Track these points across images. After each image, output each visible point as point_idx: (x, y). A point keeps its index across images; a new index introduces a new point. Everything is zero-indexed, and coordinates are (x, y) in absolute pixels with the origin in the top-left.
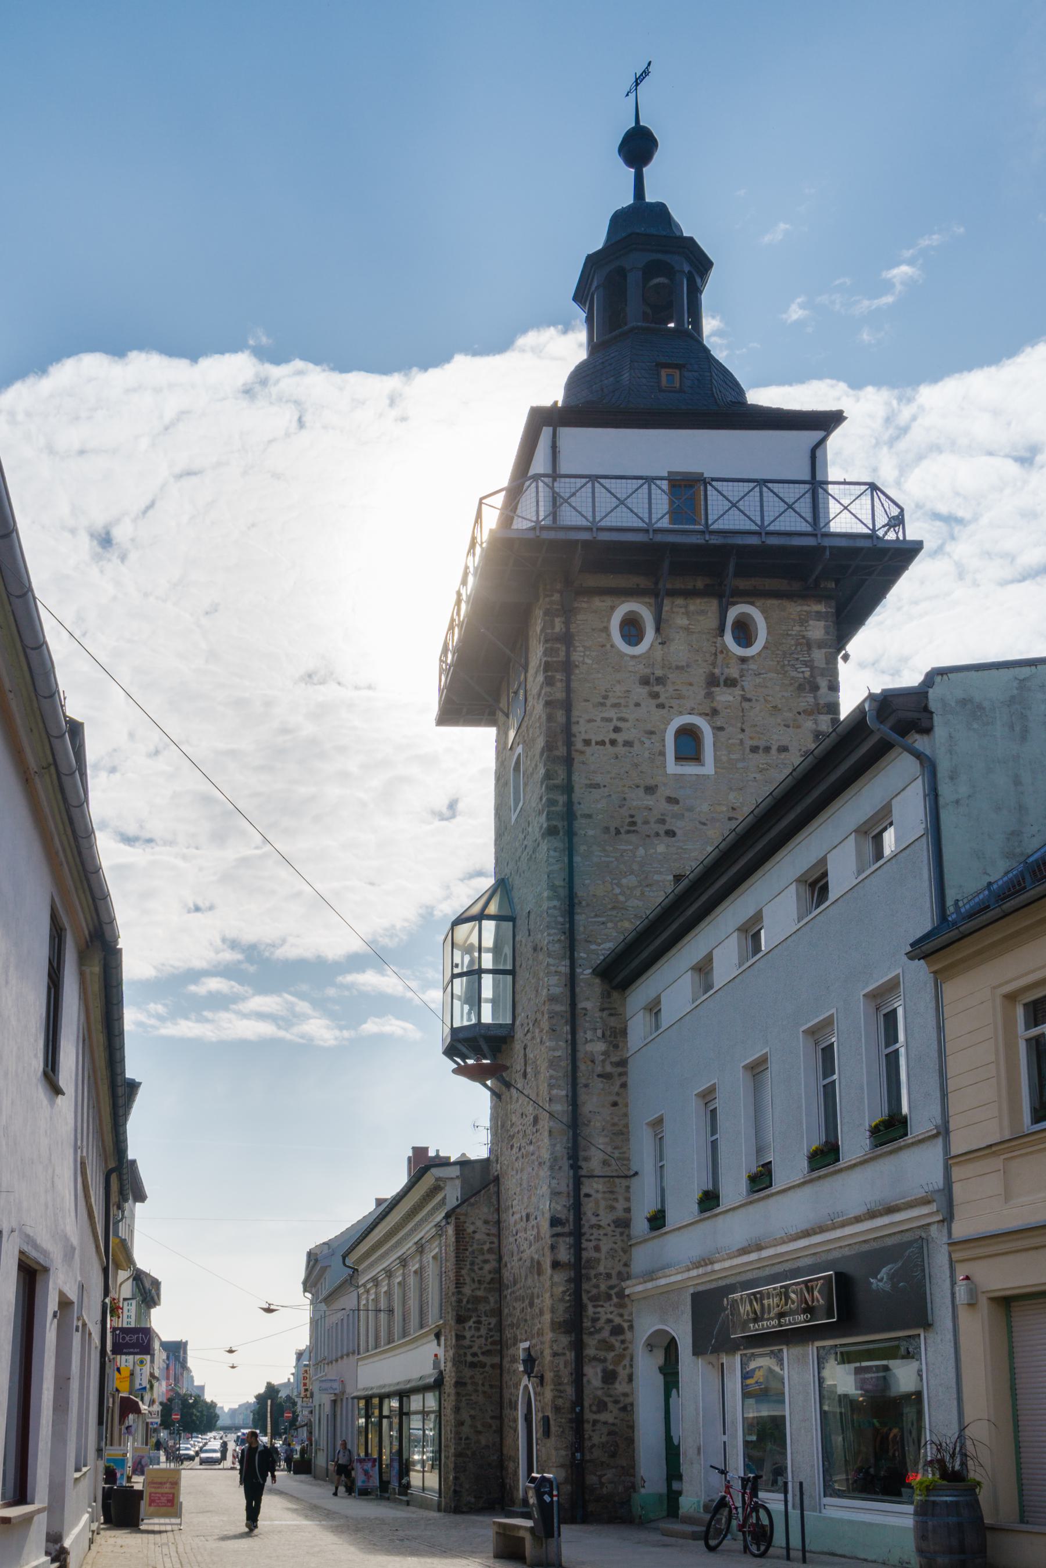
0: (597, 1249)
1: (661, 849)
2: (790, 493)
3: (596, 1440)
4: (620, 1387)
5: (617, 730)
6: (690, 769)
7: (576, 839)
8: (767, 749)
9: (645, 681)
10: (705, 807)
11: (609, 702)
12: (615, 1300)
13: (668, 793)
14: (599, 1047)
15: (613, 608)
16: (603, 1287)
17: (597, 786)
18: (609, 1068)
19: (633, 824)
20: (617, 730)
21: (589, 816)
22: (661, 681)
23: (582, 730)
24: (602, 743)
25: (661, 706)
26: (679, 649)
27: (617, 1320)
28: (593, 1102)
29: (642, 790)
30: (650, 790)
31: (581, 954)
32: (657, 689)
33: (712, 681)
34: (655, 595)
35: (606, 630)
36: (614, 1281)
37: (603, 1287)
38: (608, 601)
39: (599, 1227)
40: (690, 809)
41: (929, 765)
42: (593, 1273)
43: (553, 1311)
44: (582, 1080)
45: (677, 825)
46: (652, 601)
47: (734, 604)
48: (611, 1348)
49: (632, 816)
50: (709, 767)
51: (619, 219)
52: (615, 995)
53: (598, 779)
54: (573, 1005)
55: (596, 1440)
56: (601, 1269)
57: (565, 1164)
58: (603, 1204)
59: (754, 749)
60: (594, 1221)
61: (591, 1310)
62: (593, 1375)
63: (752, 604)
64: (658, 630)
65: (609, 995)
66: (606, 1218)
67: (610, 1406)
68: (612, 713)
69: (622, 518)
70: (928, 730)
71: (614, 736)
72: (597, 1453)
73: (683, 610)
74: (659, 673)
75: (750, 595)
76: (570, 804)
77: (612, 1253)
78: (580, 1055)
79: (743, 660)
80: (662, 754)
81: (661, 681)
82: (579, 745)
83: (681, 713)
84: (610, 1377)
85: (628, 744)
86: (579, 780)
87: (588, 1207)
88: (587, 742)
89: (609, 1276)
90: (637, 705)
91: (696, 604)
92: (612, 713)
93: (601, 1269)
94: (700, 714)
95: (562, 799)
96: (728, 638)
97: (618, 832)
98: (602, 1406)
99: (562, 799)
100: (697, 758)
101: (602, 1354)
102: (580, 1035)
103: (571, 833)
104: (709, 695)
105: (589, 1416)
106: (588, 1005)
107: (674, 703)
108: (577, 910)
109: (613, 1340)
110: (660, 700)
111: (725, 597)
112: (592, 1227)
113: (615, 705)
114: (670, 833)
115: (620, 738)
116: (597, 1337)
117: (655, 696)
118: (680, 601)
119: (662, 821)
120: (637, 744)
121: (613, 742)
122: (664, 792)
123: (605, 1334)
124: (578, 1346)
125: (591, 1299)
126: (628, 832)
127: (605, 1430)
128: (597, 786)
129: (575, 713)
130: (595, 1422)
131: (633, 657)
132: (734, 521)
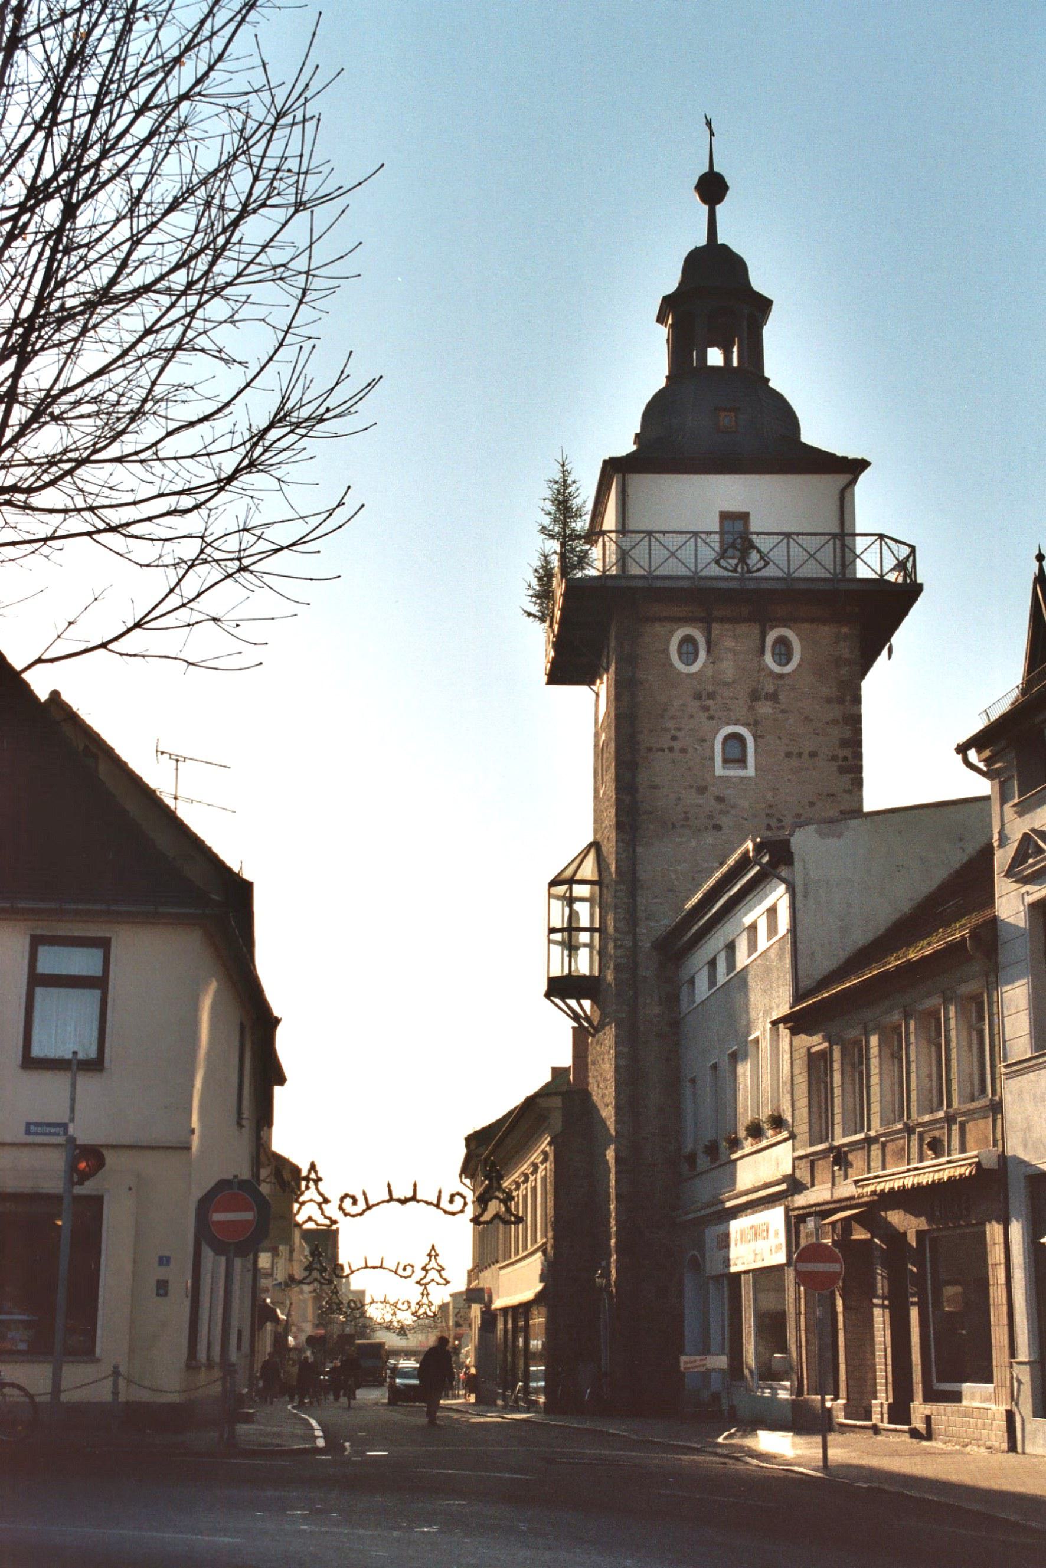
1: (710, 840)
5: (674, 738)
6: (735, 772)
8: (800, 755)
9: (698, 697)
10: (747, 805)
15: (672, 632)
19: (687, 819)
20: (674, 738)
22: (711, 696)
25: (711, 718)
29: (693, 790)
30: (702, 790)
32: (710, 703)
33: (755, 696)
34: (707, 622)
38: (668, 626)
40: (733, 807)
45: (725, 821)
46: (705, 625)
47: (772, 628)
49: (686, 813)
50: (751, 771)
51: (695, 261)
59: (789, 755)
63: (789, 627)
64: (709, 651)
73: (730, 633)
74: (710, 689)
79: (781, 676)
80: (712, 759)
81: (711, 696)
83: (728, 724)
85: (683, 750)
88: (650, 749)
90: (691, 716)
91: (742, 629)
94: (743, 725)
96: (768, 658)
100: (742, 761)
104: (751, 708)
108: (639, 892)
110: (712, 712)
111: (765, 623)
114: (718, 828)
115: (677, 745)
117: (706, 709)
118: (728, 626)
119: (711, 817)
120: (691, 750)
121: (671, 749)
126: (683, 826)
131: (688, 675)
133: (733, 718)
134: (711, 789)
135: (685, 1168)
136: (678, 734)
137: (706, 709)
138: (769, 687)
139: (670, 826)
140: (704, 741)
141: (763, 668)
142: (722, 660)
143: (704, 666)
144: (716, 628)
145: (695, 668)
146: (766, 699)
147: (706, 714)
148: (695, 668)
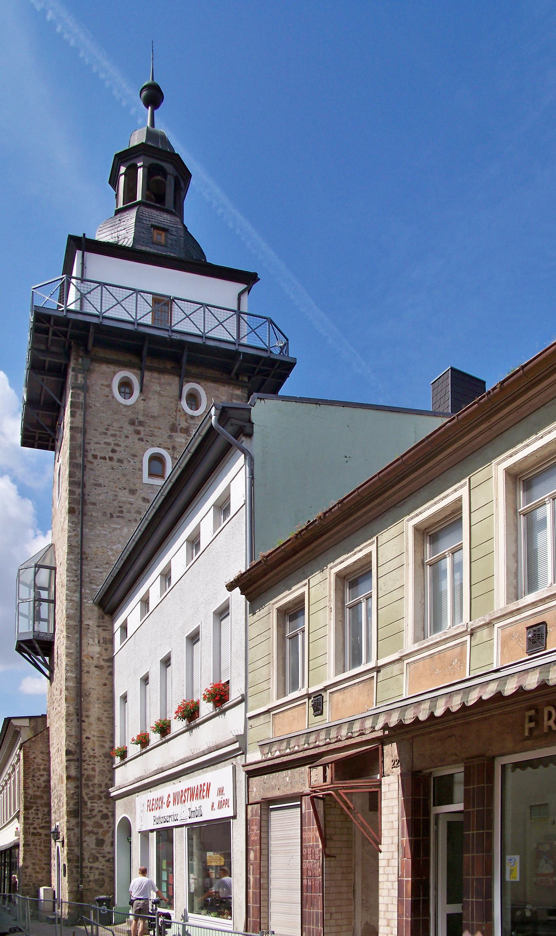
0: (93, 769)
2: (222, 315)
3: (92, 877)
4: (107, 848)
5: (113, 451)
7: (85, 518)
9: (132, 423)
11: (109, 433)
12: (104, 799)
13: (143, 495)
14: (97, 649)
15: (115, 373)
16: (97, 792)
17: (100, 485)
18: (102, 663)
19: (122, 512)
20: (113, 451)
21: (94, 504)
22: (141, 423)
23: (92, 448)
24: (104, 458)
25: (141, 440)
26: (154, 405)
27: (105, 811)
28: (92, 682)
29: (127, 490)
30: (133, 492)
31: (86, 591)
32: (140, 428)
33: (173, 428)
34: (141, 368)
35: (109, 386)
36: (103, 788)
37: (97, 792)
38: (112, 368)
39: (95, 757)
41: (251, 460)
42: (90, 783)
43: (68, 804)
44: (85, 669)
46: (139, 372)
47: (189, 382)
48: (101, 826)
49: (121, 507)
52: (107, 617)
53: (101, 481)
54: (81, 621)
55: (92, 877)
56: (96, 781)
57: (74, 717)
58: (97, 744)
60: (92, 753)
61: (89, 804)
62: (90, 841)
63: (199, 384)
64: (141, 391)
65: (103, 618)
66: (98, 752)
67: (101, 859)
68: (110, 440)
69: (118, 313)
70: (250, 435)
71: (111, 455)
72: (92, 885)
73: (157, 381)
74: (141, 418)
75: (199, 378)
76: (83, 494)
77: (102, 772)
78: (84, 653)
79: (192, 417)
80: (141, 470)
81: (141, 423)
82: (90, 458)
83: (153, 446)
84: (100, 843)
85: (120, 461)
86: (89, 482)
87: (88, 745)
88: (95, 457)
89: (100, 786)
90: (127, 437)
91: (166, 378)
92: (110, 440)
93: (96, 781)
94: (165, 448)
95: (79, 491)
97: (112, 516)
98: (96, 859)
99: (79, 491)
101: (95, 830)
102: (84, 641)
103: (83, 514)
104: (170, 437)
105: (86, 863)
106: (90, 623)
107: (150, 439)
109: (102, 822)
110: (141, 436)
111: (183, 376)
112: (90, 757)
113: (114, 435)
115: (116, 456)
116: (94, 820)
117: (138, 433)
118: (156, 375)
120: (125, 462)
121: (111, 459)
122: (141, 493)
123: (98, 818)
124: (81, 825)
125: (89, 798)
126: (118, 517)
127: (97, 872)
128: (100, 485)
129: (88, 436)
130: (91, 868)
131: (126, 406)
132: (186, 326)
133: (158, 443)
134: (139, 492)
135: (118, 760)
136: (117, 448)
137: (138, 433)
138: (184, 424)
139: (109, 516)
140: (135, 456)
141: (178, 410)
142: (150, 399)
143: (137, 401)
144: (147, 374)
145: (130, 402)
146: (181, 432)
147: (138, 436)
148: (130, 402)
